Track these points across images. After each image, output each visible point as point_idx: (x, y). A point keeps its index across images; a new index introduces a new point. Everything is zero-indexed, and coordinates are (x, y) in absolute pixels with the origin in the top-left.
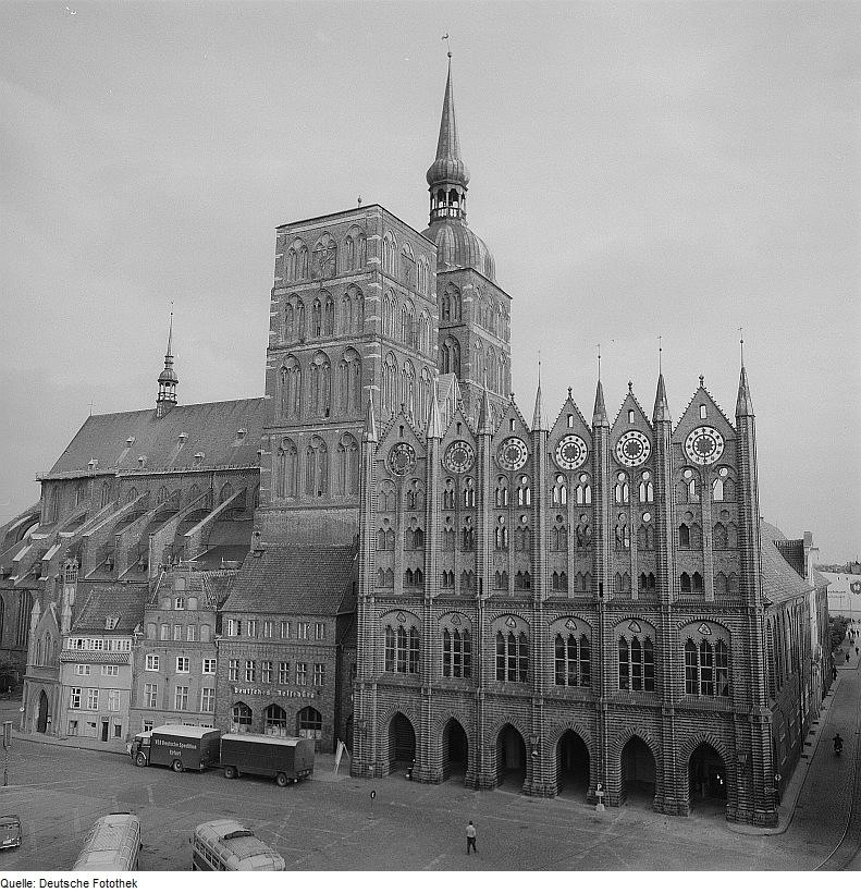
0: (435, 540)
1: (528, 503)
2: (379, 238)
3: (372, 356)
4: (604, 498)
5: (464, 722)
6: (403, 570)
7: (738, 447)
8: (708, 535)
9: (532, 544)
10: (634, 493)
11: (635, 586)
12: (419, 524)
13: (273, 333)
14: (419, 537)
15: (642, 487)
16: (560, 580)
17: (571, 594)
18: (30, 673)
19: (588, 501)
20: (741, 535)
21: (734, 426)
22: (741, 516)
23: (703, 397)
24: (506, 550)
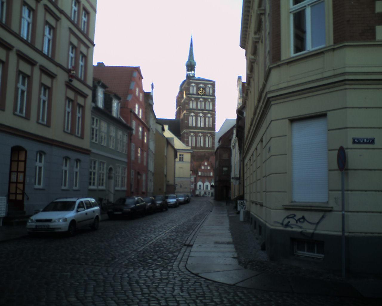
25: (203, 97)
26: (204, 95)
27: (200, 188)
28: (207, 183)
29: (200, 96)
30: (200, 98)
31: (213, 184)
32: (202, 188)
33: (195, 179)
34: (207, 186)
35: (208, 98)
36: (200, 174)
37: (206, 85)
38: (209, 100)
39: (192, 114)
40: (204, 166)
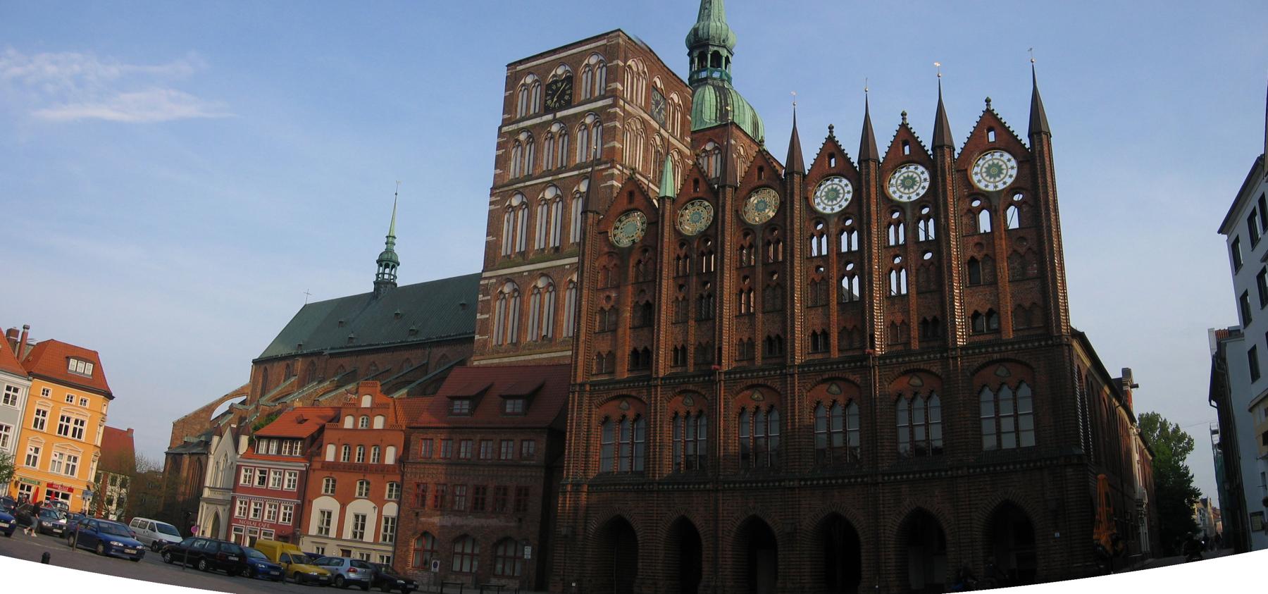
0: (665, 313)
1: (780, 258)
2: (621, 64)
3: (609, 183)
4: (875, 239)
5: (698, 521)
6: (628, 350)
7: (1033, 167)
8: (1004, 269)
9: (784, 305)
10: (912, 232)
11: (915, 333)
12: (648, 297)
13: (498, 171)
14: (647, 314)
15: (922, 224)
16: (819, 339)
17: (835, 354)
18: (206, 493)
19: (855, 247)
20: (1042, 263)
21: (1028, 146)
22: (1040, 236)
23: (990, 120)
24: (751, 316)
25: (559, 115)
26: (569, 105)
27: (323, 530)
28: (362, 506)
29: (550, 117)
30: (549, 123)
31: (391, 509)
32: (333, 533)
33: (304, 478)
34: (361, 520)
35: (583, 115)
36: (330, 453)
37: (575, 61)
38: (589, 120)
39: (516, 201)
40: (357, 411)
